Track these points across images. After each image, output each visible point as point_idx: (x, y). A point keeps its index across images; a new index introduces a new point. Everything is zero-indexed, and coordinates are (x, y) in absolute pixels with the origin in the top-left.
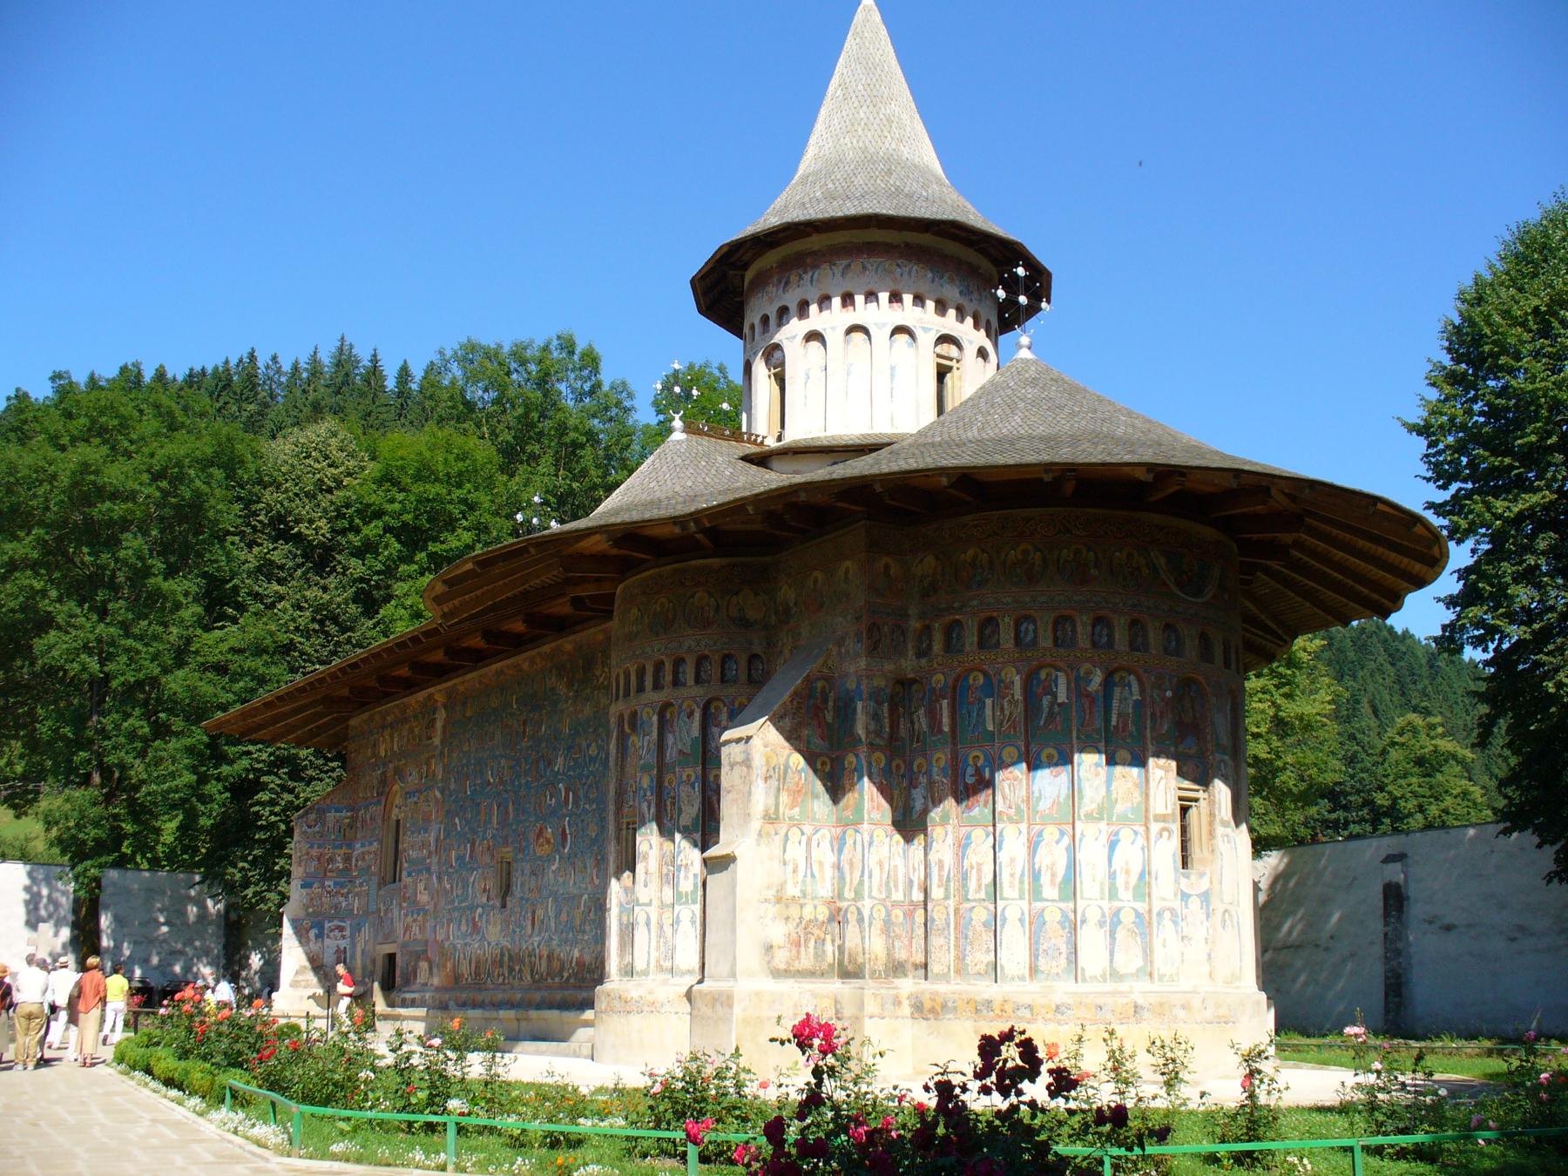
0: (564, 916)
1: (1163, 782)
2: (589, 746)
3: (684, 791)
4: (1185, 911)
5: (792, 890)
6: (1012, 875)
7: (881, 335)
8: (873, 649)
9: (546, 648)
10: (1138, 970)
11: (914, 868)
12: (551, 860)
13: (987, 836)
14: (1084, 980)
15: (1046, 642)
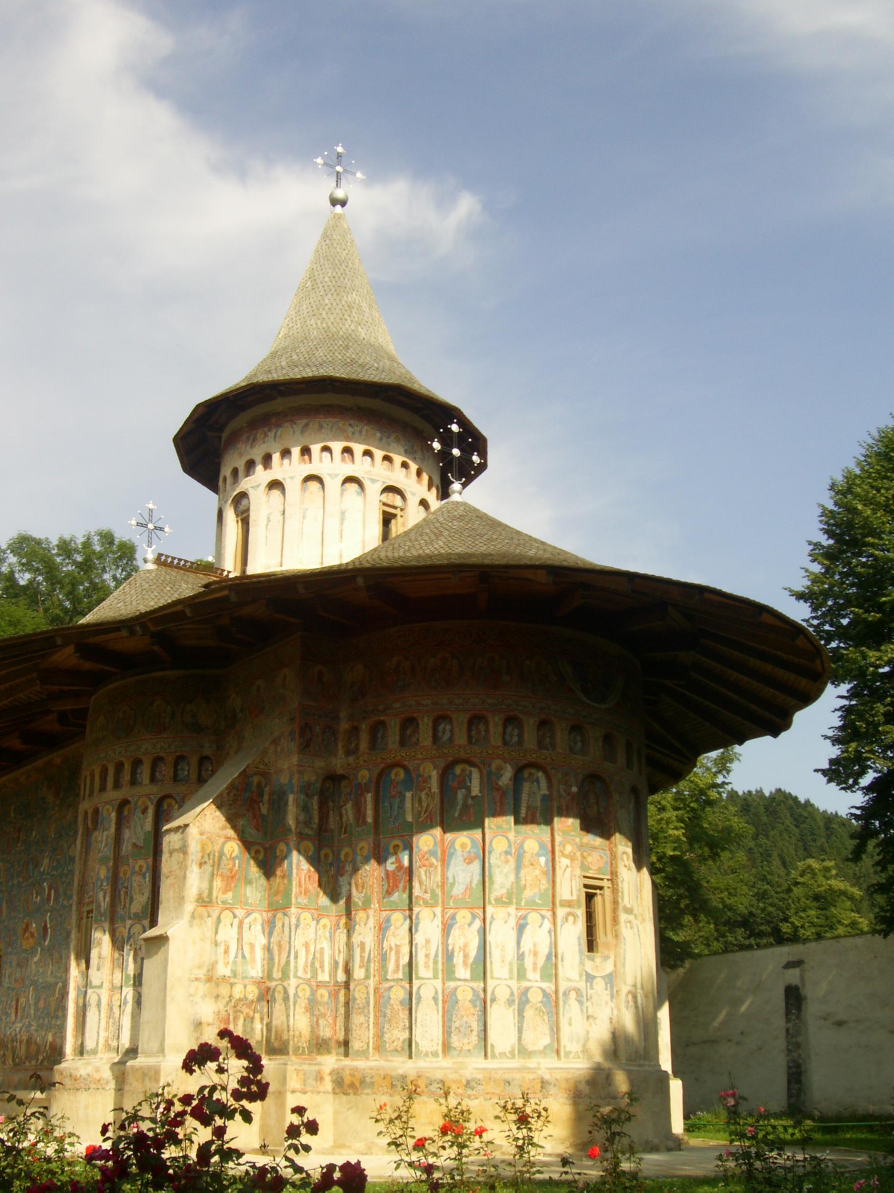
0: (41, 1004)
1: (569, 870)
3: (136, 880)
4: (590, 992)
5: (223, 970)
6: (427, 956)
7: (333, 485)
8: (305, 746)
9: (40, 763)
10: (545, 1047)
11: (339, 950)
12: (33, 952)
13: (405, 920)
14: (494, 1056)
15: (461, 739)
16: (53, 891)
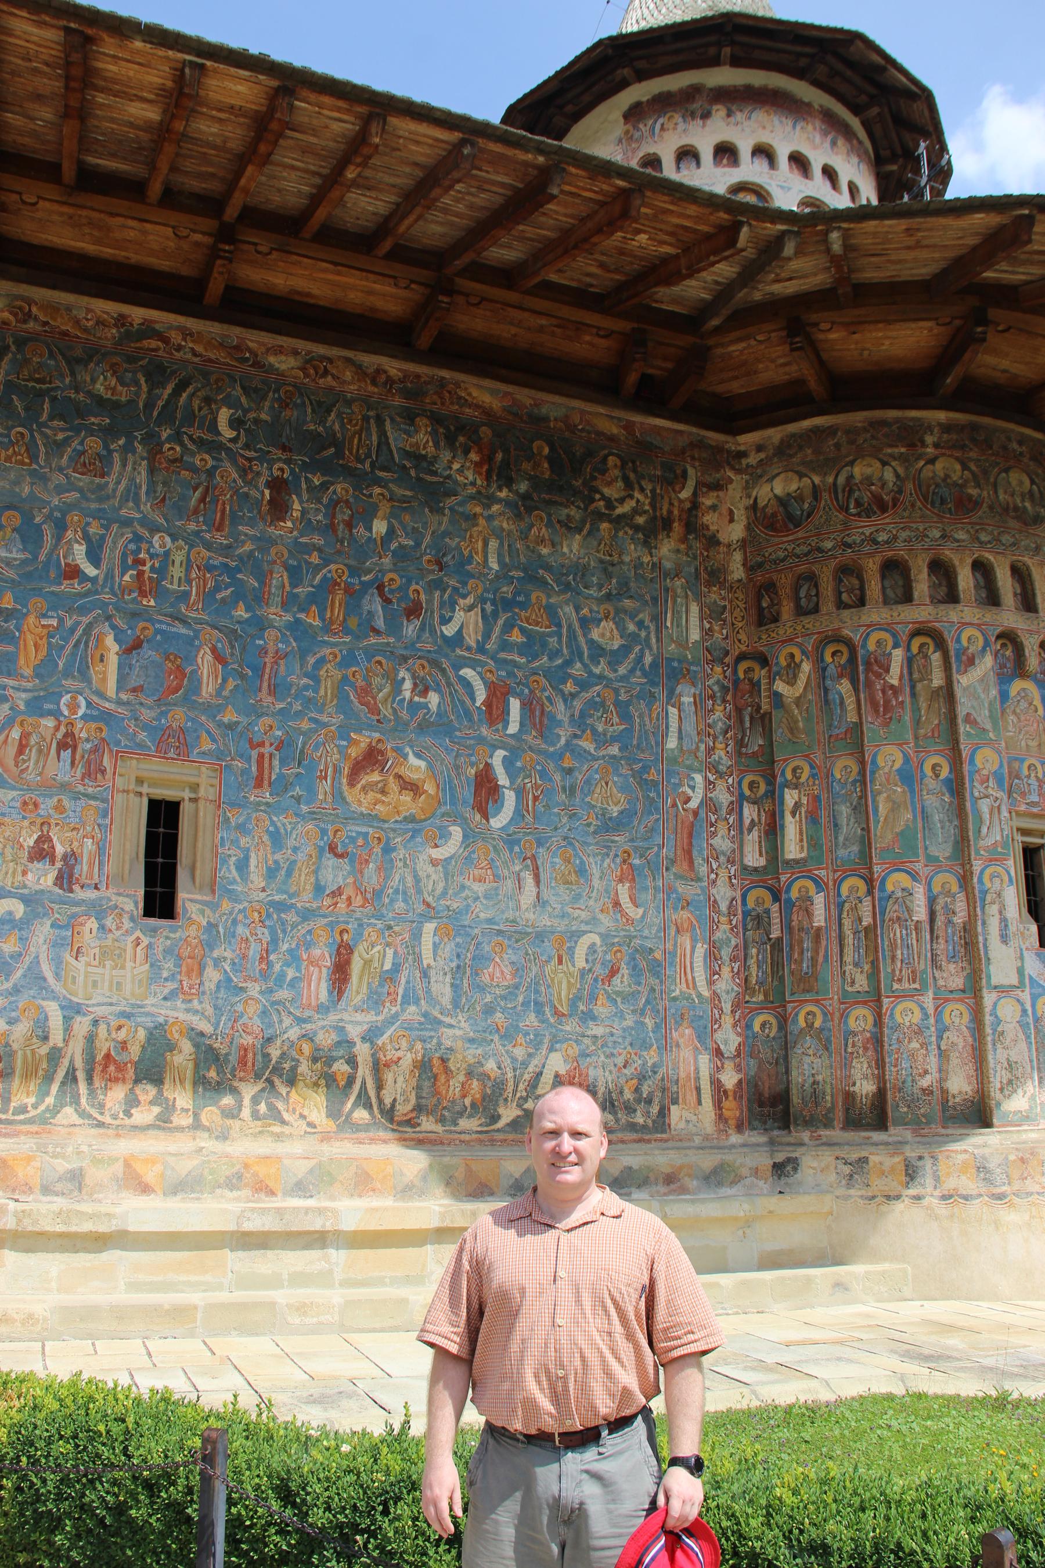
2: (585, 623)
16: (515, 705)
